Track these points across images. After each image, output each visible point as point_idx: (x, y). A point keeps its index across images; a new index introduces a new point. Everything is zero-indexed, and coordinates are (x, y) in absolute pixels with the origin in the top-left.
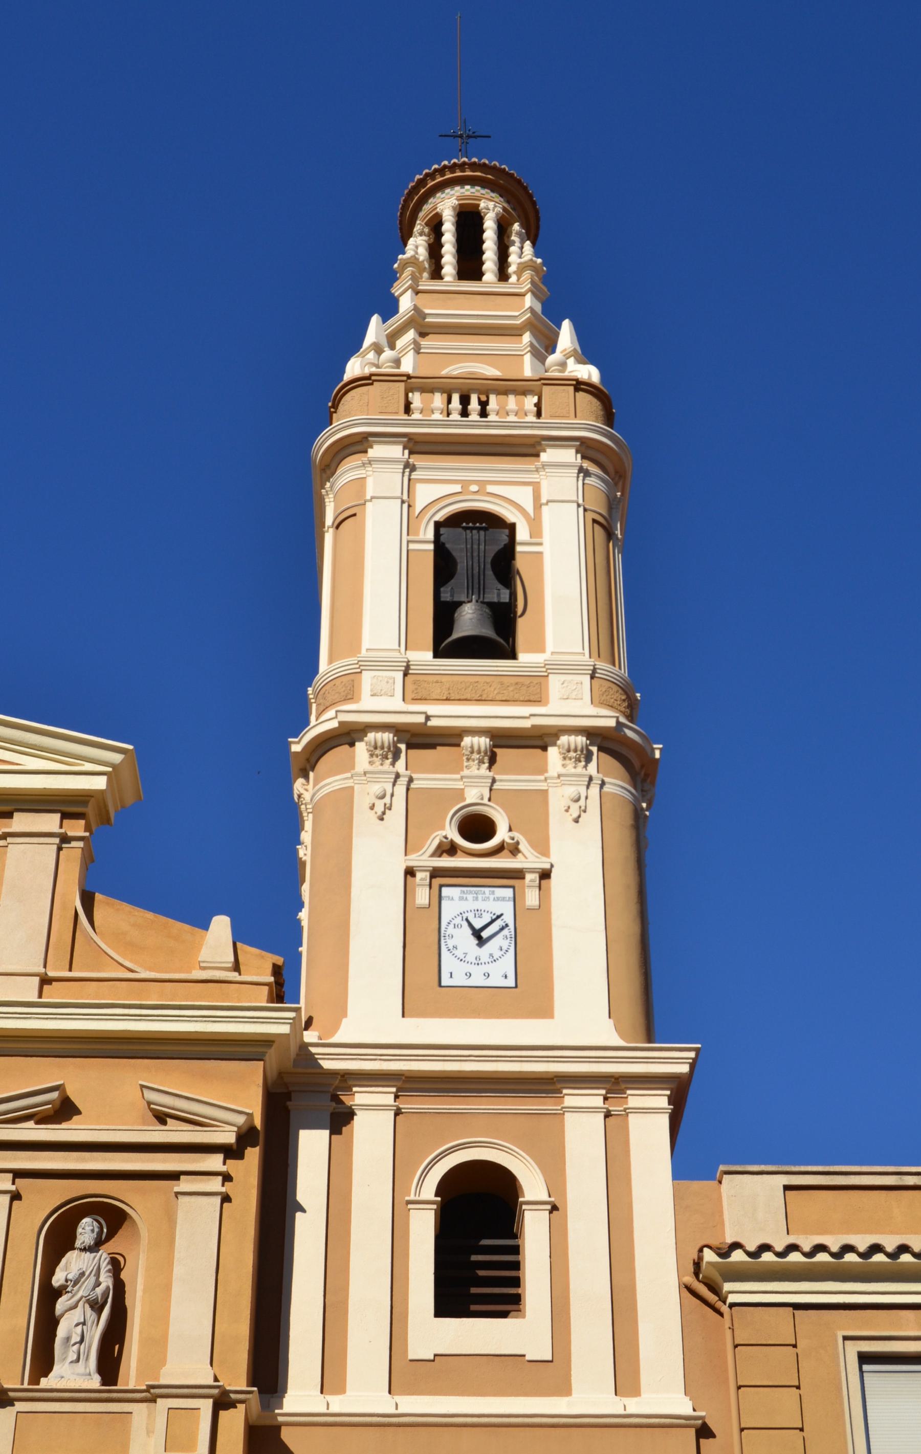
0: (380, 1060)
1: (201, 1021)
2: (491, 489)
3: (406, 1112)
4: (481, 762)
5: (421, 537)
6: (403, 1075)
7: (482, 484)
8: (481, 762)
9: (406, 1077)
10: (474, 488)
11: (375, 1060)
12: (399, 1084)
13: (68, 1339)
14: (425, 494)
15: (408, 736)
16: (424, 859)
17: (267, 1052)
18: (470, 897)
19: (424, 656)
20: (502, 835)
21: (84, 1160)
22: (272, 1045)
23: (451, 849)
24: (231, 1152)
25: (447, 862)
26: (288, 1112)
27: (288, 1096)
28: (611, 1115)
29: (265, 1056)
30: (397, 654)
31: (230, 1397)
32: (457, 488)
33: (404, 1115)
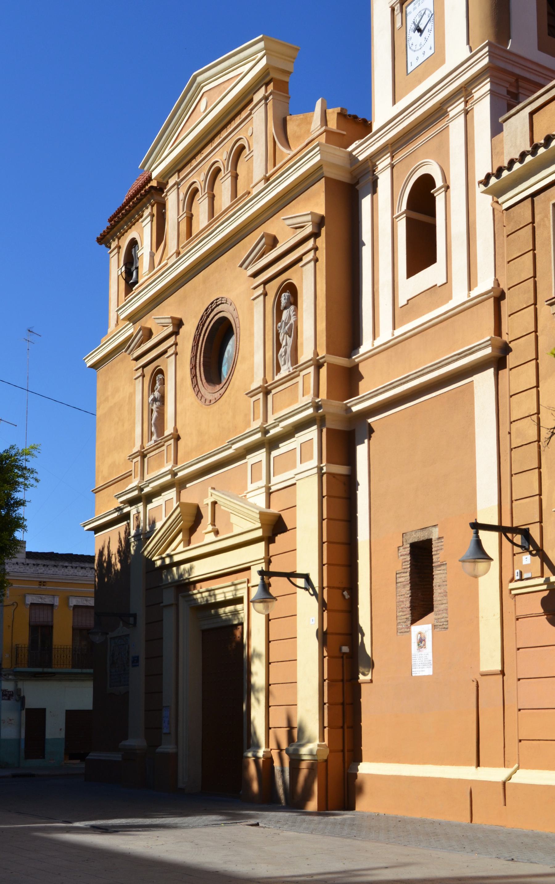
0: (376, 142)
1: (294, 173)
3: (396, 164)
6: (388, 145)
9: (391, 144)
11: (375, 143)
12: (390, 149)
13: (281, 355)
17: (323, 172)
21: (279, 266)
22: (322, 167)
24: (315, 235)
26: (357, 191)
28: (469, 112)
29: (323, 174)
31: (320, 362)
33: (396, 166)
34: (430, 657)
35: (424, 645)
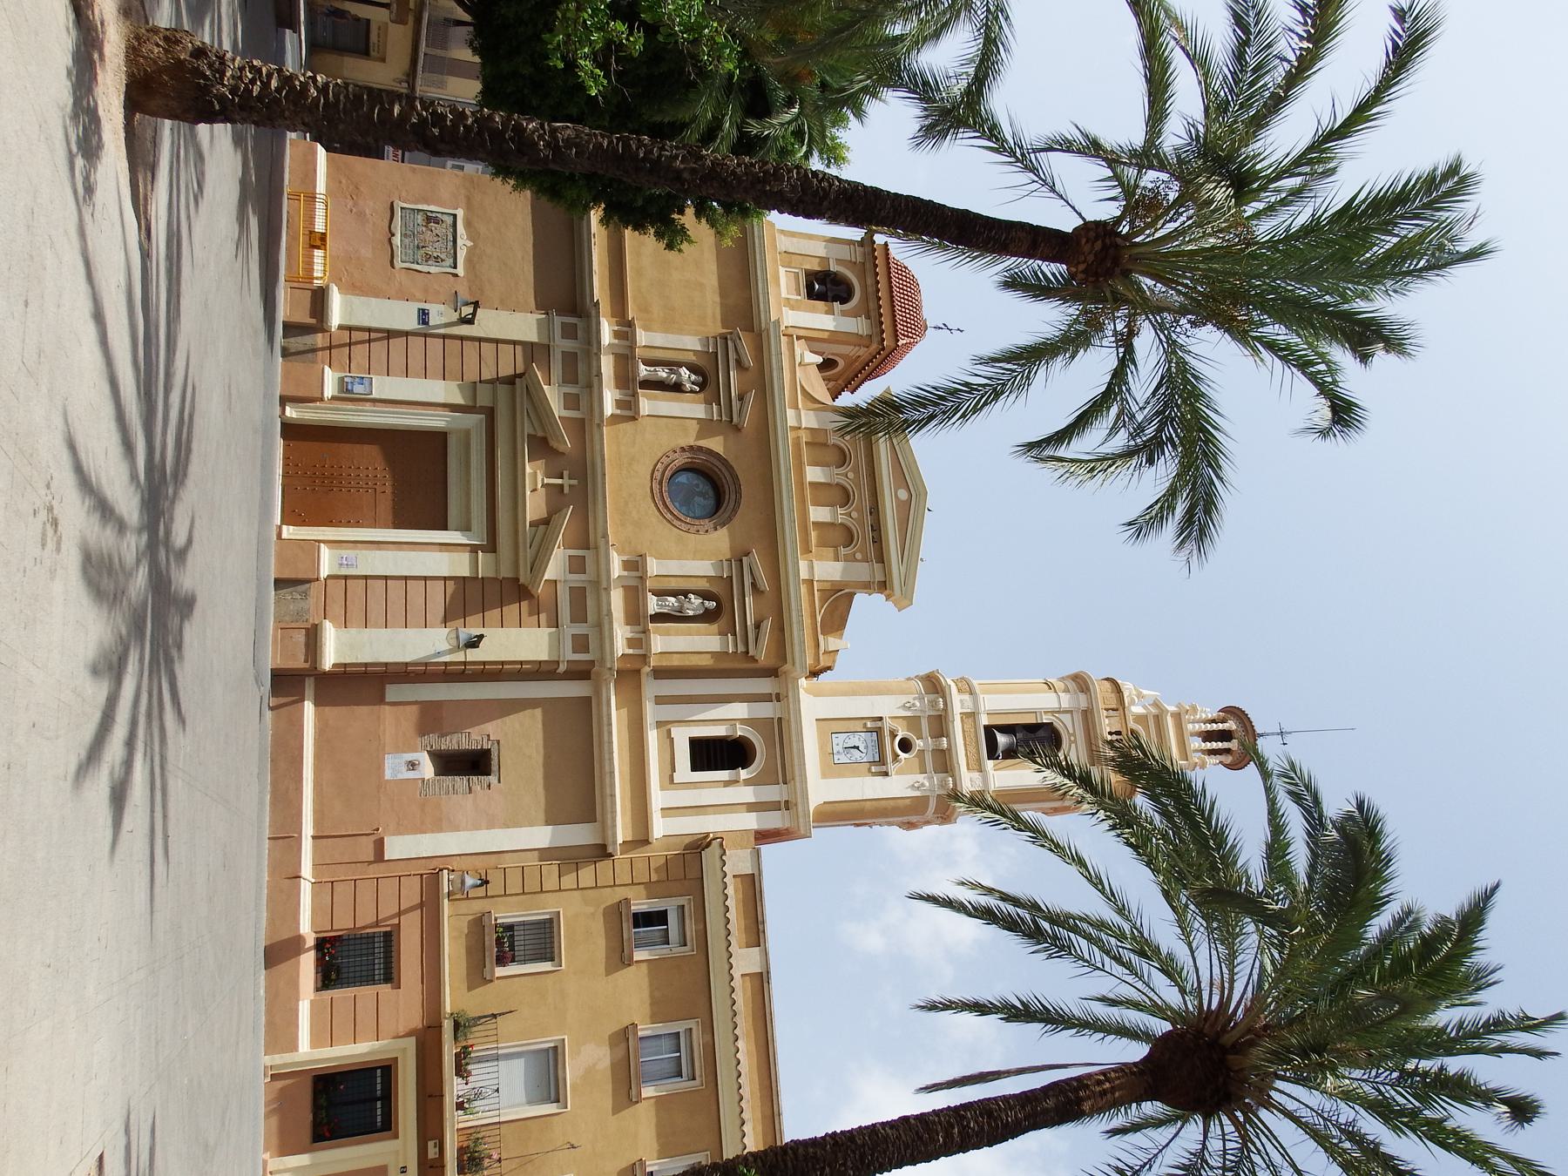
2: (1073, 745)
4: (936, 745)
5: (1044, 717)
7: (1075, 741)
8: (936, 745)
10: (1072, 738)
14: (1066, 718)
15: (943, 714)
16: (887, 725)
18: (873, 744)
19: (985, 720)
20: (903, 755)
23: (893, 735)
25: (887, 733)
27: (777, 676)
30: (983, 709)
32: (1071, 731)
34: (400, 777)
35: (410, 770)
